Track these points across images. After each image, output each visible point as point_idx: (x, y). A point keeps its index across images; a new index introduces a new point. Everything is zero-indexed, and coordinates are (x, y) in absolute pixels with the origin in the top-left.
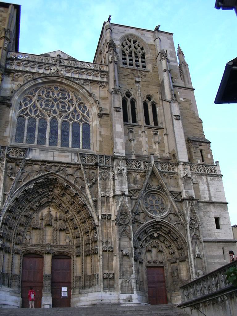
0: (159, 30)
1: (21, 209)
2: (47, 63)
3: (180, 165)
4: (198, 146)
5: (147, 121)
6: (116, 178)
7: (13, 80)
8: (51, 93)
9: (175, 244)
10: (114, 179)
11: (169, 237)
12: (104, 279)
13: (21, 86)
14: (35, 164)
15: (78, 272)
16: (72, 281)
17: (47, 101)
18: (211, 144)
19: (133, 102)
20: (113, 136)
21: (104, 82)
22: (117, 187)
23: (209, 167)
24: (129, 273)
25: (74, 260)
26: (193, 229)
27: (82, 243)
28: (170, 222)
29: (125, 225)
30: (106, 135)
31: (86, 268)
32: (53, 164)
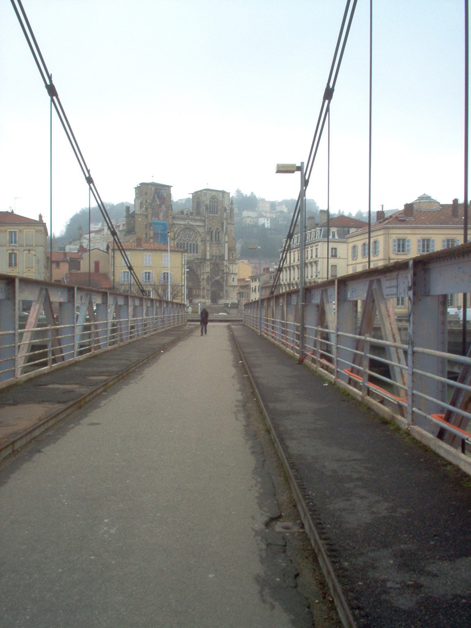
10: (206, 267)
17: (185, 235)
19: (212, 232)
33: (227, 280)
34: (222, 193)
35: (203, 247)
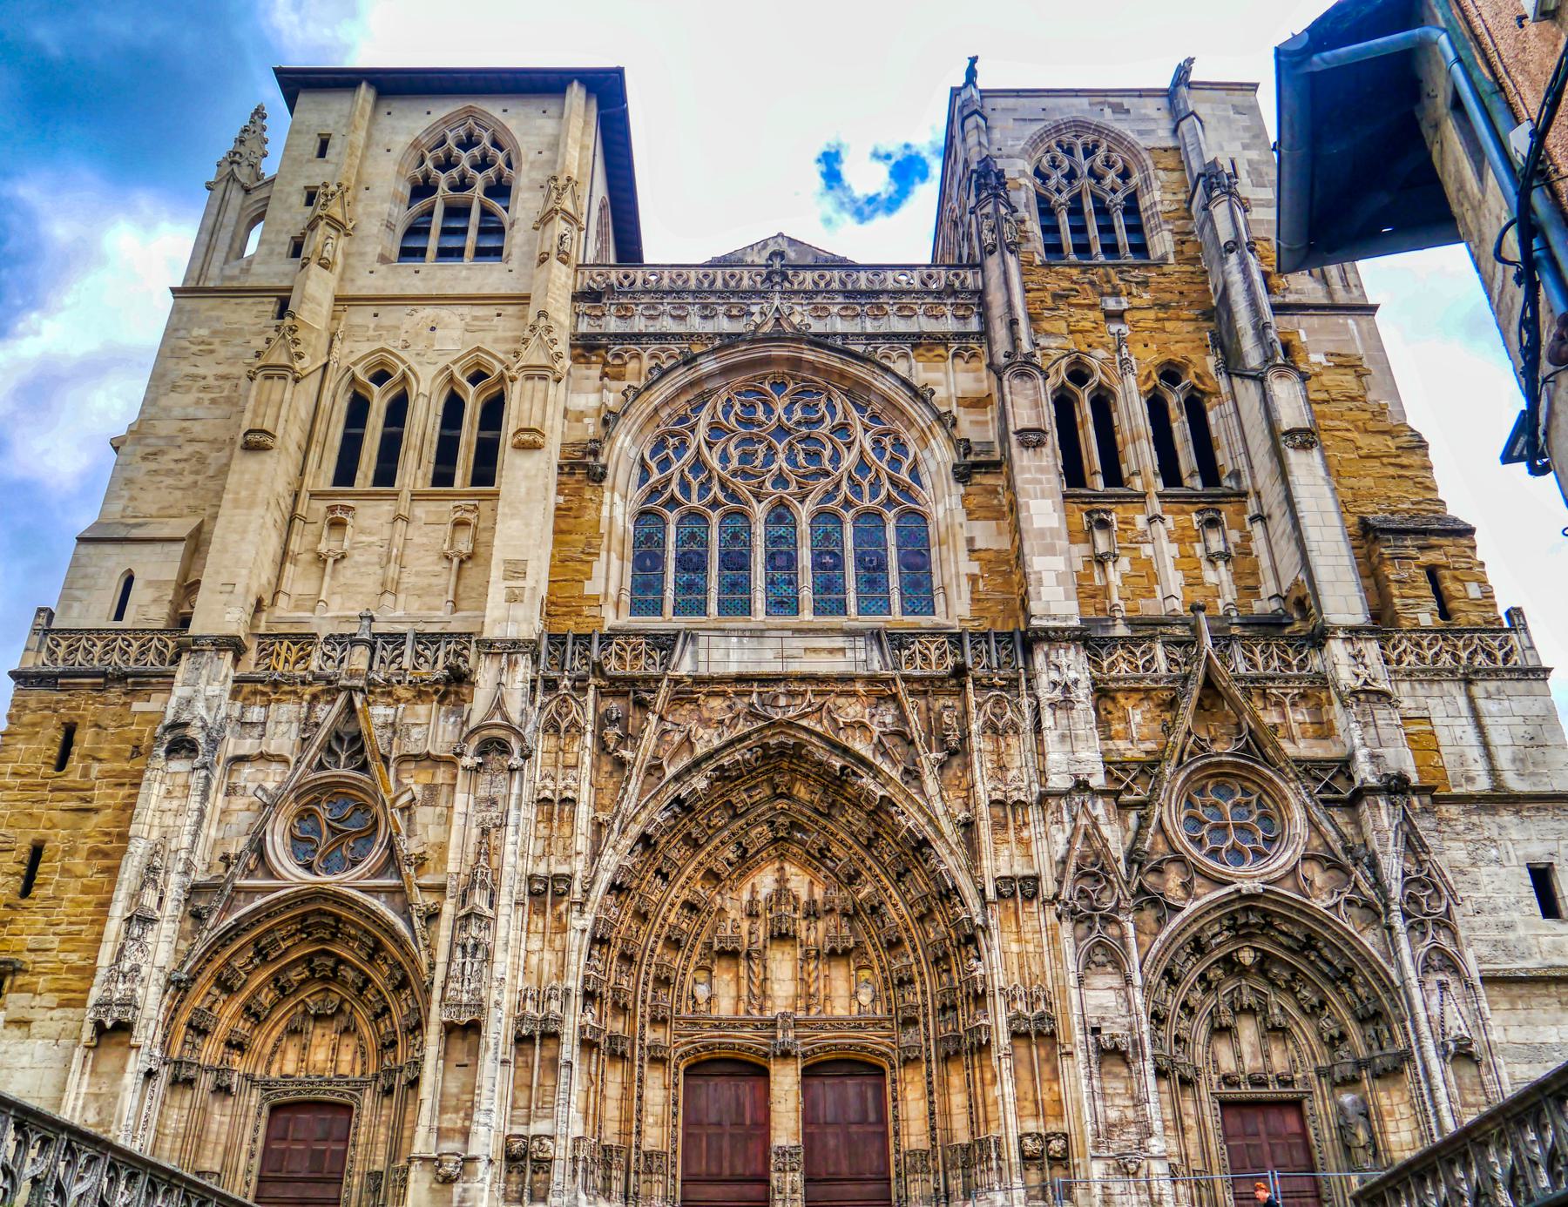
0: (1192, 78)
1: (665, 877)
2: (733, 293)
3: (1331, 642)
4: (1413, 552)
5: (1169, 470)
6: (1048, 720)
7: (604, 375)
8: (761, 408)
9: (1342, 994)
10: (1038, 728)
11: (1312, 963)
12: (1027, 1159)
13: (638, 394)
14: (709, 695)
15: (914, 1135)
16: (893, 1175)
18: (1476, 536)
20: (1020, 549)
21: (966, 335)
22: (1056, 756)
23: (1476, 641)
24: (1133, 1129)
25: (894, 1081)
26: (1422, 923)
27: (925, 1005)
28: (1308, 897)
29: (1102, 917)
30: (995, 547)
31: (947, 1114)
32: (781, 689)
33: (1423, 882)
34: (1163, 102)
35: (987, 535)
